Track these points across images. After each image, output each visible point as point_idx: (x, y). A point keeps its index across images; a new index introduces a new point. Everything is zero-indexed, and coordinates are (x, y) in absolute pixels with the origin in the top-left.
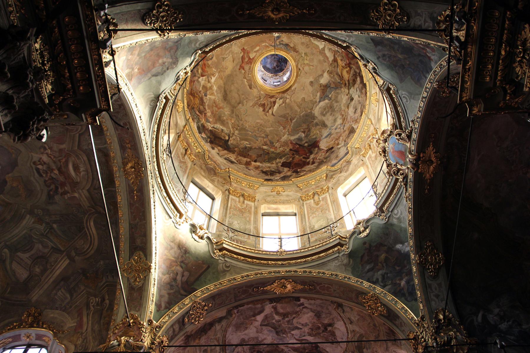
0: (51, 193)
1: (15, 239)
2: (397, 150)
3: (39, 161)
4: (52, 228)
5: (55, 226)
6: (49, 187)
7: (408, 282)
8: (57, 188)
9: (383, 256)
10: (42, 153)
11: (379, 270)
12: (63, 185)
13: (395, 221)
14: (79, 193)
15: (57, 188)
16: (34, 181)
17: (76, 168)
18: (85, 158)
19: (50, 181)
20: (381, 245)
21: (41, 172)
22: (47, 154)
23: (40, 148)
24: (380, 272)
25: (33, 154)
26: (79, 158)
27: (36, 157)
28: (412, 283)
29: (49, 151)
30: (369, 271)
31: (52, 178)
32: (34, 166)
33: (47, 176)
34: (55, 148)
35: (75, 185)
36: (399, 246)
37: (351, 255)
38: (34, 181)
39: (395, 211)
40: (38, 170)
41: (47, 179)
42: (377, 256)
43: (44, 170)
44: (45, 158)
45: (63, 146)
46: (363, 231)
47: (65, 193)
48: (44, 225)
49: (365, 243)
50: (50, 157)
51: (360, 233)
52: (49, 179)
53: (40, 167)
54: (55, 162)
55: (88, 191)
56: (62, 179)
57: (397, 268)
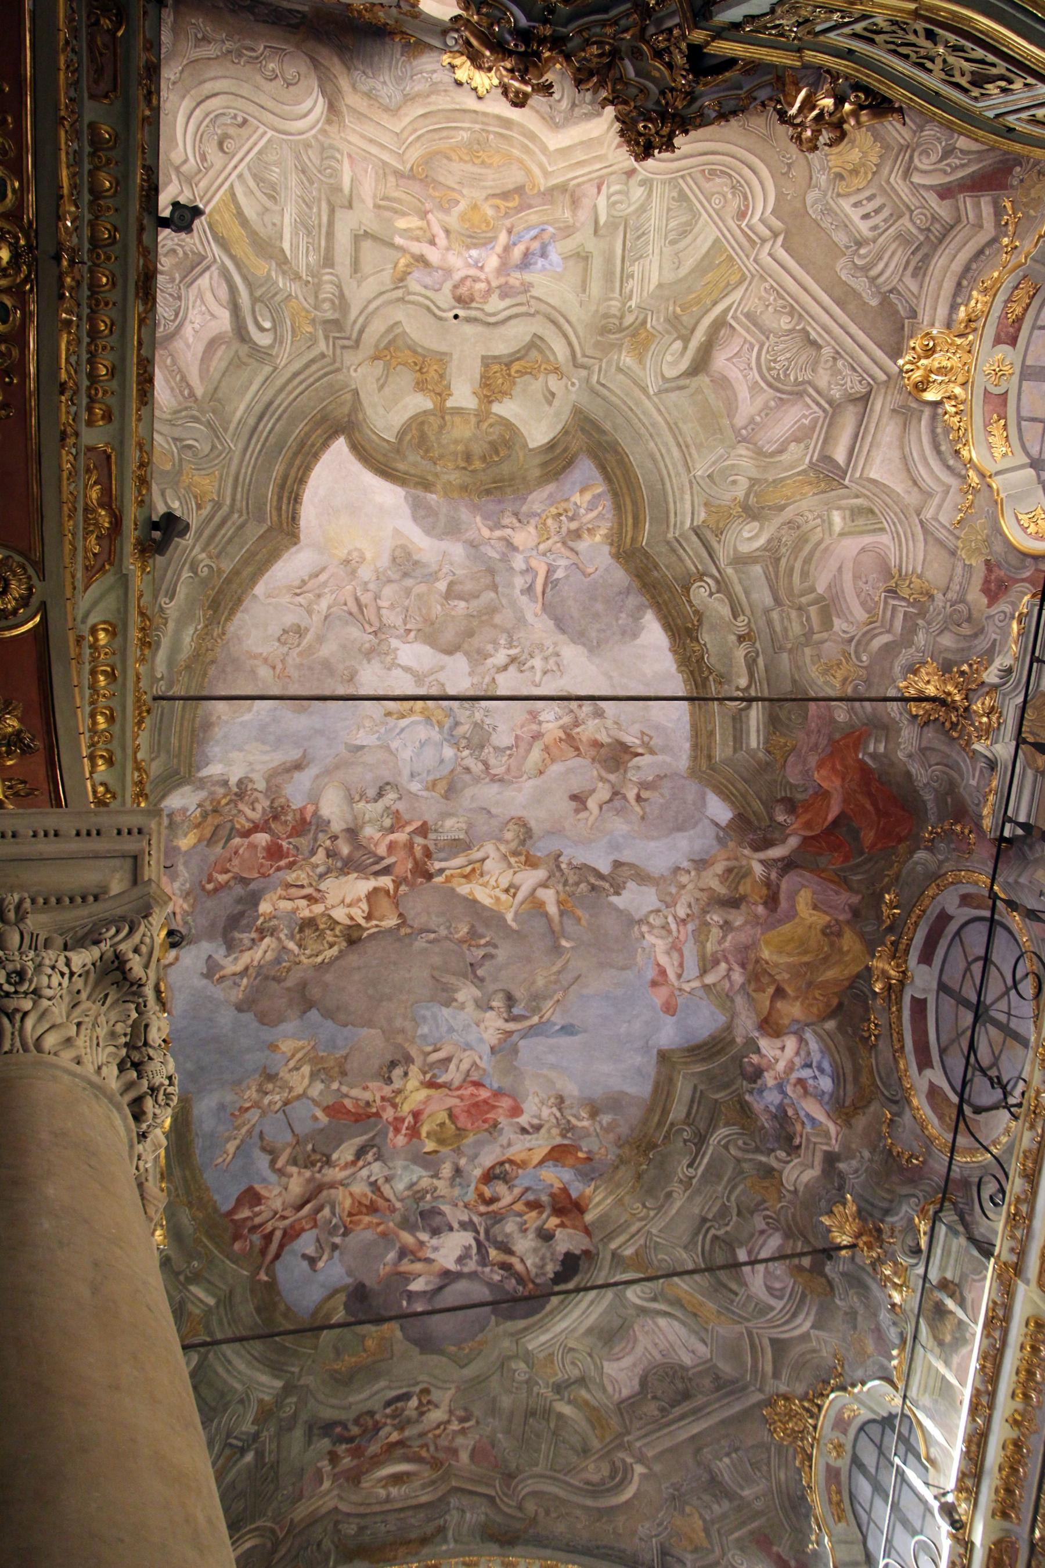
0: (338, 1430)
1: (220, 1370)
3: (429, 1402)
4: (243, 1451)
5: (249, 1457)
6: (357, 1421)
8: (351, 1440)
10: (451, 1412)
12: (357, 1452)
14: (329, 1491)
15: (351, 1440)
16: (376, 1387)
17: (398, 1479)
18: (423, 1499)
19: (370, 1422)
21: (400, 1405)
22: (448, 1422)
23: (466, 1409)
25: (453, 1391)
26: (424, 1486)
27: (444, 1397)
29: (455, 1426)
31: (377, 1428)
32: (417, 1389)
33: (387, 1416)
34: (460, 1441)
35: (354, 1478)
38: (376, 1387)
40: (406, 1397)
41: (377, 1417)
43: (403, 1410)
44: (436, 1415)
45: (464, 1457)
47: (334, 1458)
48: (253, 1429)
50: (438, 1426)
52: (376, 1423)
53: (414, 1402)
54: (422, 1435)
55: (336, 1508)
56: (374, 1448)
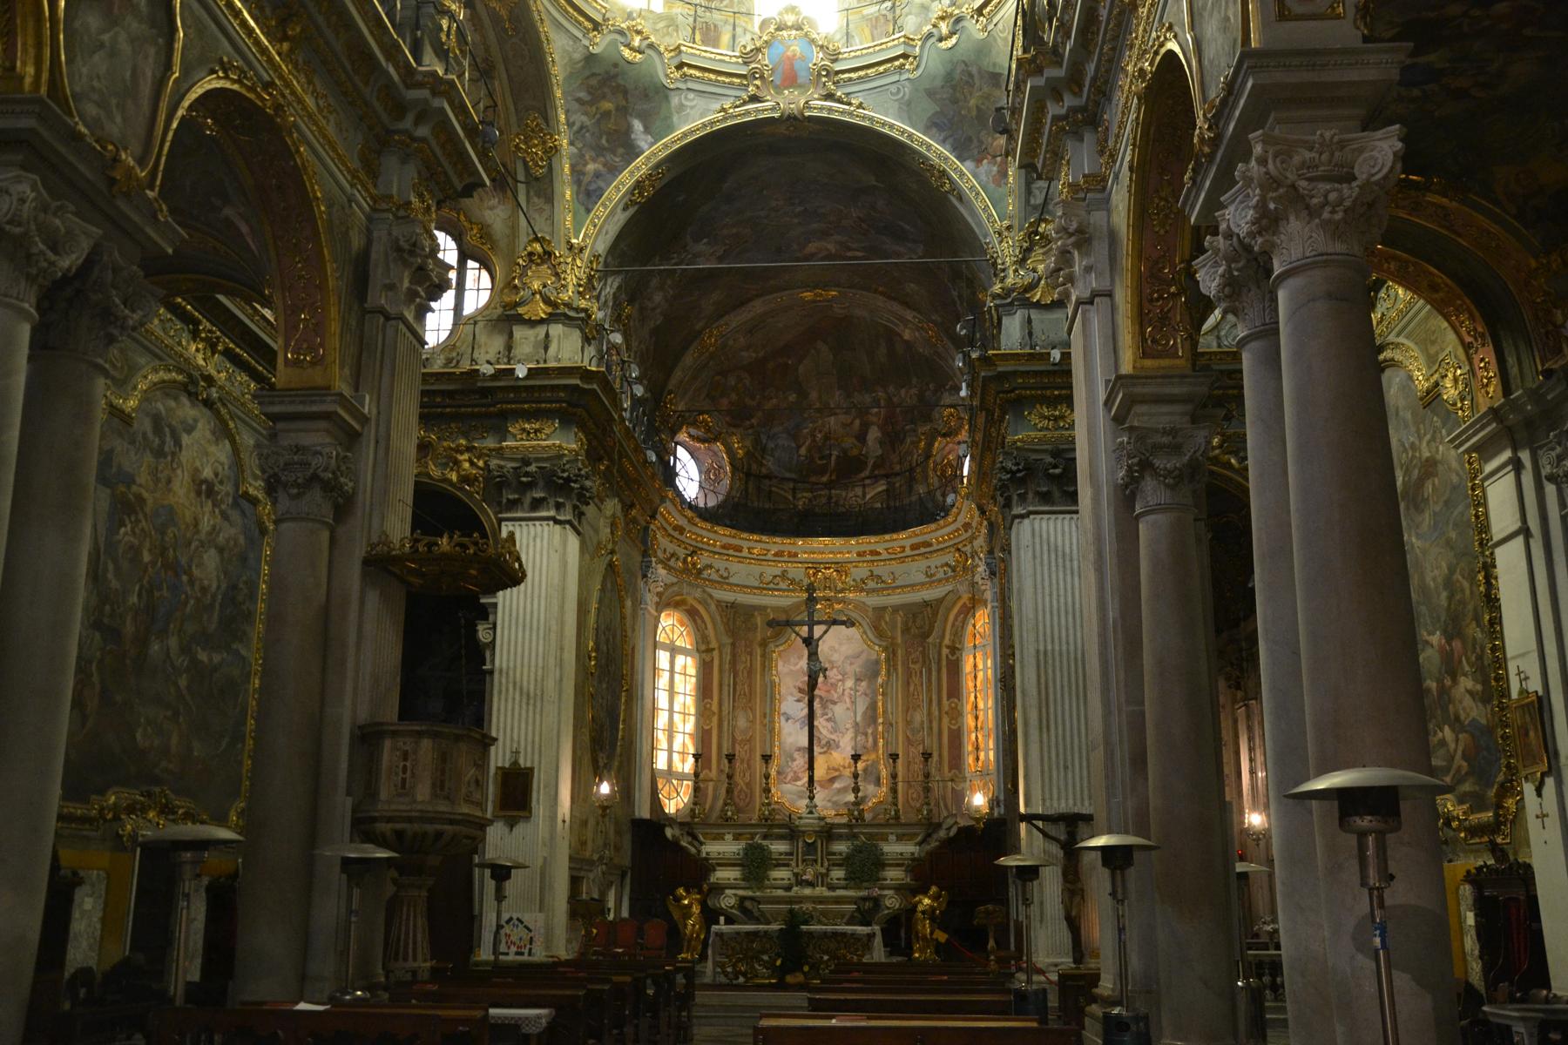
2: (797, 67)
7: (597, 175)
9: (607, 105)
11: (586, 114)
13: (675, 101)
20: (625, 92)
24: (584, 118)
28: (601, 183)
30: (578, 100)
36: (638, 126)
37: (590, 58)
39: (691, 95)
42: (604, 97)
46: (632, 49)
49: (616, 65)
51: (628, 46)
57: (604, 141)
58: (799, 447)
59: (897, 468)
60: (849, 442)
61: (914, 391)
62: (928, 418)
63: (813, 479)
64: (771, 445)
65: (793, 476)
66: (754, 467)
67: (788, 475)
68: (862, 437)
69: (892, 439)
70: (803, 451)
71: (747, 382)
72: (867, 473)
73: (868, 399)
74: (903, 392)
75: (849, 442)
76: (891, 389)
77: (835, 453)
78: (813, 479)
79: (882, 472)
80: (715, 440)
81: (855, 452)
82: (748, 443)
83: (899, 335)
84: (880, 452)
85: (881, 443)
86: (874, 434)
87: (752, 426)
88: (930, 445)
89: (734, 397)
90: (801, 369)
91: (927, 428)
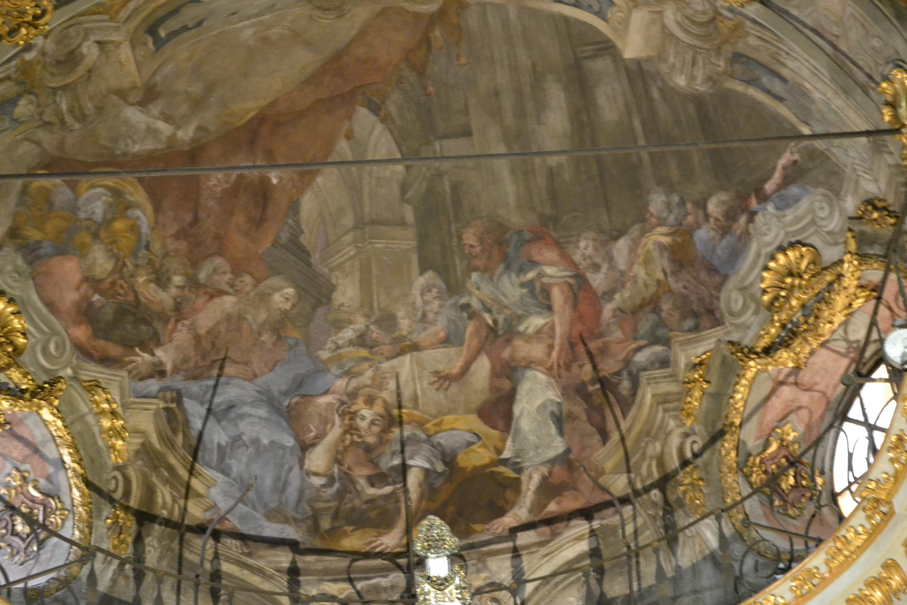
58: (305, 447)
59: (619, 484)
60: (460, 428)
61: (660, 236)
62: (705, 314)
63: (353, 541)
64: (217, 435)
65: (291, 532)
66: (164, 495)
67: (272, 530)
68: (499, 410)
69: (598, 398)
70: (318, 459)
71: (144, 217)
72: (520, 513)
73: (510, 288)
74: (622, 246)
75: (460, 428)
76: (584, 248)
77: (418, 463)
78: (353, 541)
79: (570, 503)
80: (41, 392)
81: (480, 456)
82: (145, 420)
83: (607, 48)
84: (558, 446)
85: (559, 420)
86: (536, 395)
87: (159, 372)
88: (720, 399)
89: (101, 262)
90: (308, 204)
91: (704, 346)
